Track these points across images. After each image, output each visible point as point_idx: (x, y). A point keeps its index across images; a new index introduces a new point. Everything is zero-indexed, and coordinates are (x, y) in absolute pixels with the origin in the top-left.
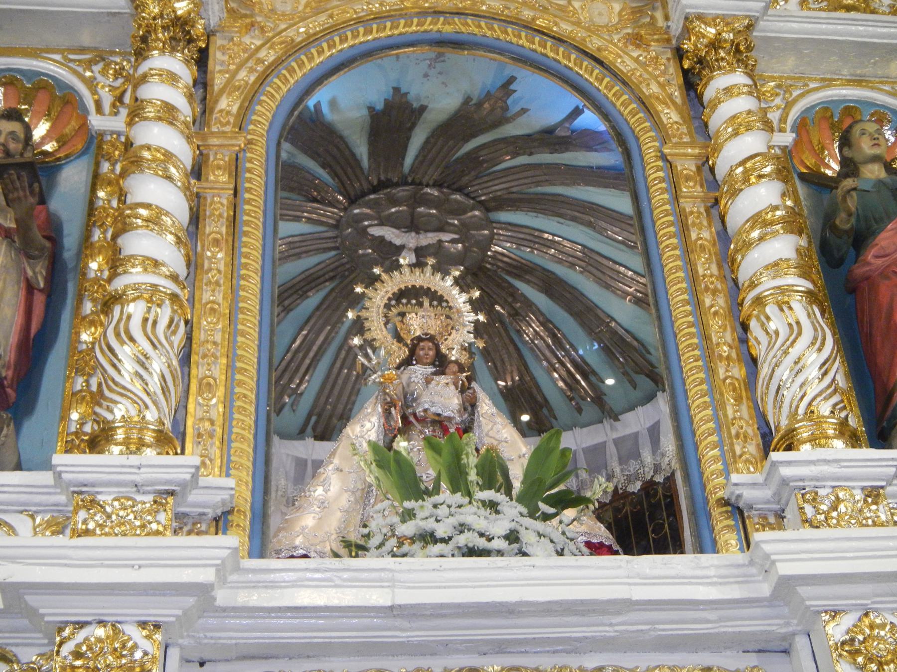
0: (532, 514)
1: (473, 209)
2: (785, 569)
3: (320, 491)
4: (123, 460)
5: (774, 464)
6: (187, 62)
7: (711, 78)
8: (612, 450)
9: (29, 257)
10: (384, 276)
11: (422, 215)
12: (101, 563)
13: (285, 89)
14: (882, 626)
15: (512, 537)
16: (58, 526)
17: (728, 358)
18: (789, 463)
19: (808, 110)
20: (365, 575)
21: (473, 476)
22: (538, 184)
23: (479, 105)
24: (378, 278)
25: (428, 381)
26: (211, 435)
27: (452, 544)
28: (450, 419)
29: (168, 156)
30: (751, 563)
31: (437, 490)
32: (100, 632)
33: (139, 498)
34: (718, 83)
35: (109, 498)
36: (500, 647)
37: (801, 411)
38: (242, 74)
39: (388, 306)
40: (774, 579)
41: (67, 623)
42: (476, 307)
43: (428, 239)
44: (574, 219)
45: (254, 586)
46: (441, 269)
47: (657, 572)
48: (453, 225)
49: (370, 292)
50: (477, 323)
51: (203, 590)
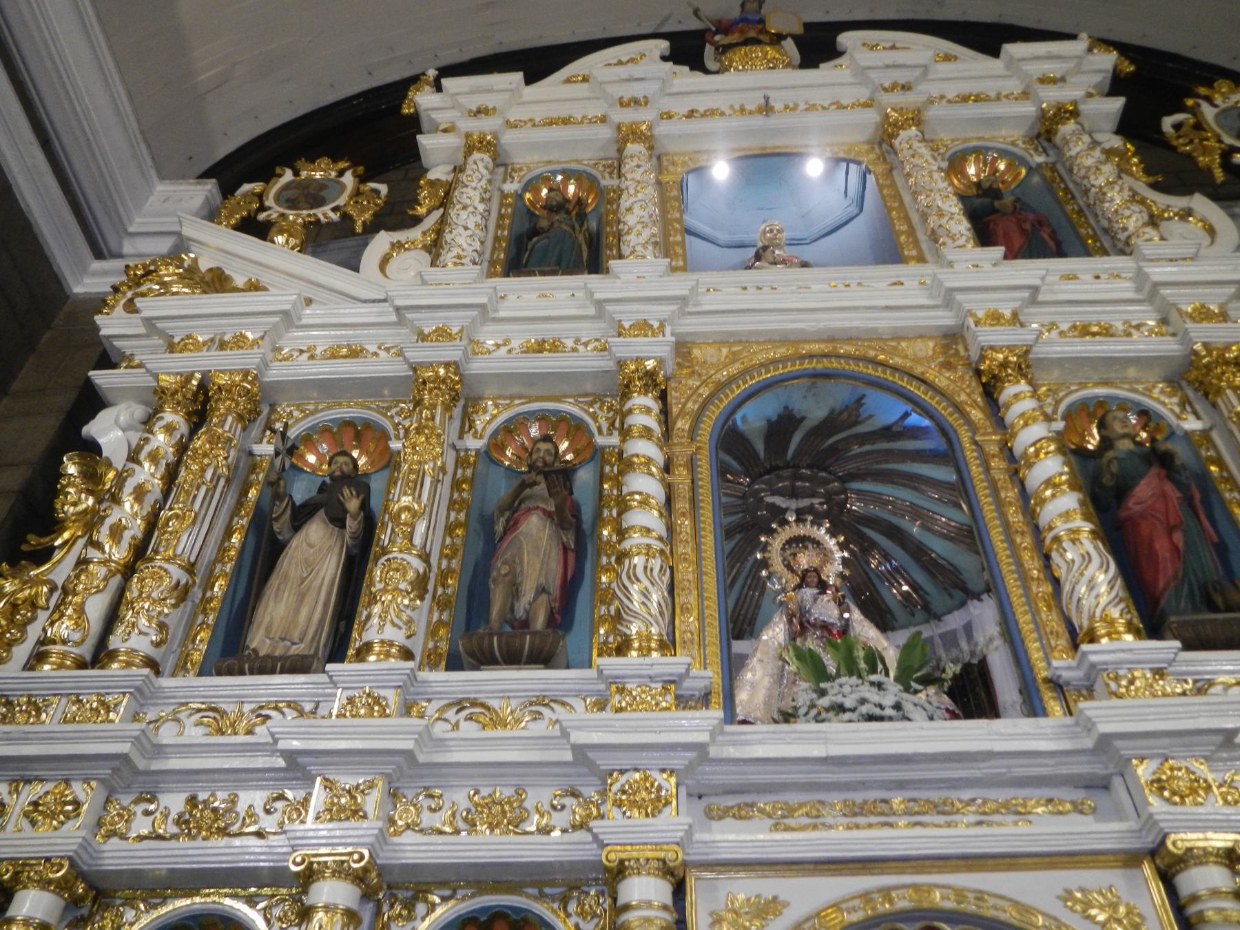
0: (907, 689)
1: (834, 481)
2: (1104, 728)
3: (749, 675)
4: (641, 660)
5: (1085, 654)
6: (655, 398)
7: (1003, 388)
8: (938, 641)
9: (563, 529)
10: (779, 529)
12: (636, 730)
13: (718, 413)
14: (1180, 769)
15: (898, 707)
16: (601, 705)
17: (1038, 579)
18: (1095, 652)
19: (1071, 405)
20: (806, 736)
21: (863, 665)
22: (878, 463)
23: (841, 413)
24: (775, 531)
25: (815, 600)
26: (692, 642)
27: (857, 713)
28: (832, 624)
29: (649, 461)
30: (1077, 724)
31: (838, 675)
32: (637, 776)
33: (653, 685)
34: (1008, 392)
35: (634, 686)
37: (1098, 614)
38: (690, 405)
39: (783, 549)
40: (1095, 736)
41: (614, 770)
42: (842, 547)
43: (804, 503)
44: (904, 485)
45: (734, 744)
46: (817, 523)
47: (1009, 731)
49: (770, 540)
50: (843, 558)
51: (701, 748)
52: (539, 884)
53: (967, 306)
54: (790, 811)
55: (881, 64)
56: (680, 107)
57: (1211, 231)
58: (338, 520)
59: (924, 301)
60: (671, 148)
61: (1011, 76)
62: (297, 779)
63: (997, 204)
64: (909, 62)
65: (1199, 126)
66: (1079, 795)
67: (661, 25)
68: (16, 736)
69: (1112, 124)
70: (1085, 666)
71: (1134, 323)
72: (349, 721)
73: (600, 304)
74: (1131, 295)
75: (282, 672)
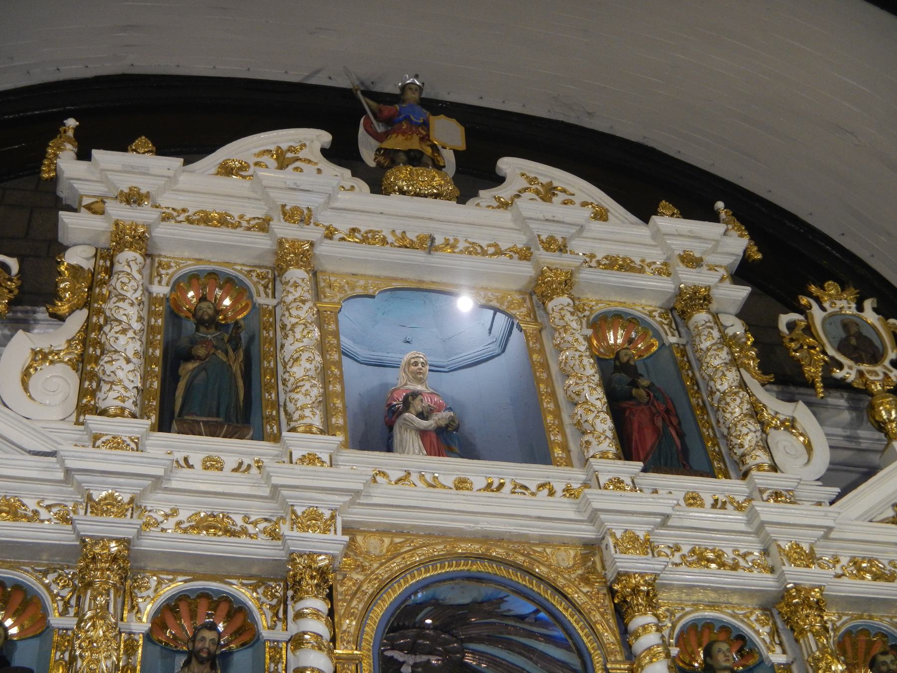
1: (455, 642)
7: (633, 617)
11: (420, 644)
19: (684, 626)
34: (638, 621)
38: (354, 603)
44: (520, 654)
48: (439, 651)
53: (608, 525)
55: (541, 216)
56: (343, 226)
57: (808, 447)
59: (572, 515)
60: (329, 267)
61: (656, 246)
63: (634, 391)
64: (567, 220)
65: (809, 330)
67: (309, 77)
69: (735, 309)
71: (742, 551)
73: (275, 488)
74: (742, 527)
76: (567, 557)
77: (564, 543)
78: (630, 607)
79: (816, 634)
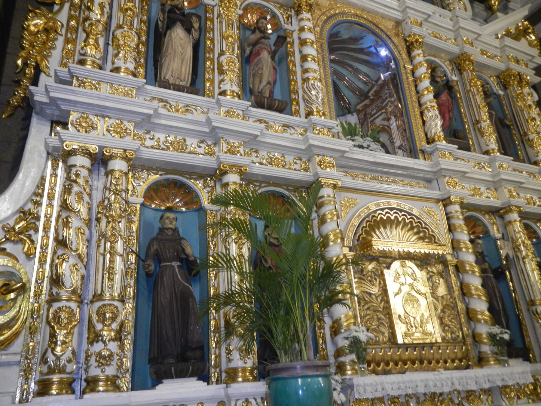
36: (386, 173)
51: (345, 152)
52: (287, 186)
53: (409, 15)
54: (357, 176)
58: (188, 30)
62: (210, 137)
66: (425, 183)
68: (102, 97)
70: (435, 148)
72: (228, 118)
74: (451, 28)
75: (187, 92)
76: (390, 25)
77: (390, 19)
78: (414, 47)
79: (471, 71)
